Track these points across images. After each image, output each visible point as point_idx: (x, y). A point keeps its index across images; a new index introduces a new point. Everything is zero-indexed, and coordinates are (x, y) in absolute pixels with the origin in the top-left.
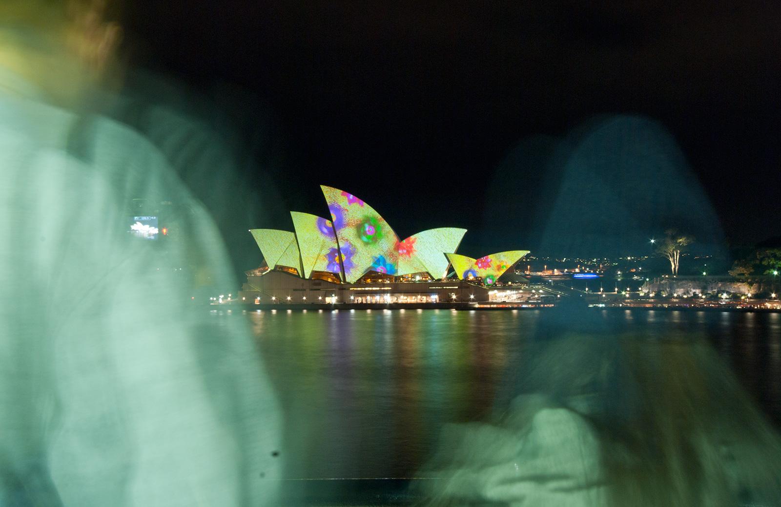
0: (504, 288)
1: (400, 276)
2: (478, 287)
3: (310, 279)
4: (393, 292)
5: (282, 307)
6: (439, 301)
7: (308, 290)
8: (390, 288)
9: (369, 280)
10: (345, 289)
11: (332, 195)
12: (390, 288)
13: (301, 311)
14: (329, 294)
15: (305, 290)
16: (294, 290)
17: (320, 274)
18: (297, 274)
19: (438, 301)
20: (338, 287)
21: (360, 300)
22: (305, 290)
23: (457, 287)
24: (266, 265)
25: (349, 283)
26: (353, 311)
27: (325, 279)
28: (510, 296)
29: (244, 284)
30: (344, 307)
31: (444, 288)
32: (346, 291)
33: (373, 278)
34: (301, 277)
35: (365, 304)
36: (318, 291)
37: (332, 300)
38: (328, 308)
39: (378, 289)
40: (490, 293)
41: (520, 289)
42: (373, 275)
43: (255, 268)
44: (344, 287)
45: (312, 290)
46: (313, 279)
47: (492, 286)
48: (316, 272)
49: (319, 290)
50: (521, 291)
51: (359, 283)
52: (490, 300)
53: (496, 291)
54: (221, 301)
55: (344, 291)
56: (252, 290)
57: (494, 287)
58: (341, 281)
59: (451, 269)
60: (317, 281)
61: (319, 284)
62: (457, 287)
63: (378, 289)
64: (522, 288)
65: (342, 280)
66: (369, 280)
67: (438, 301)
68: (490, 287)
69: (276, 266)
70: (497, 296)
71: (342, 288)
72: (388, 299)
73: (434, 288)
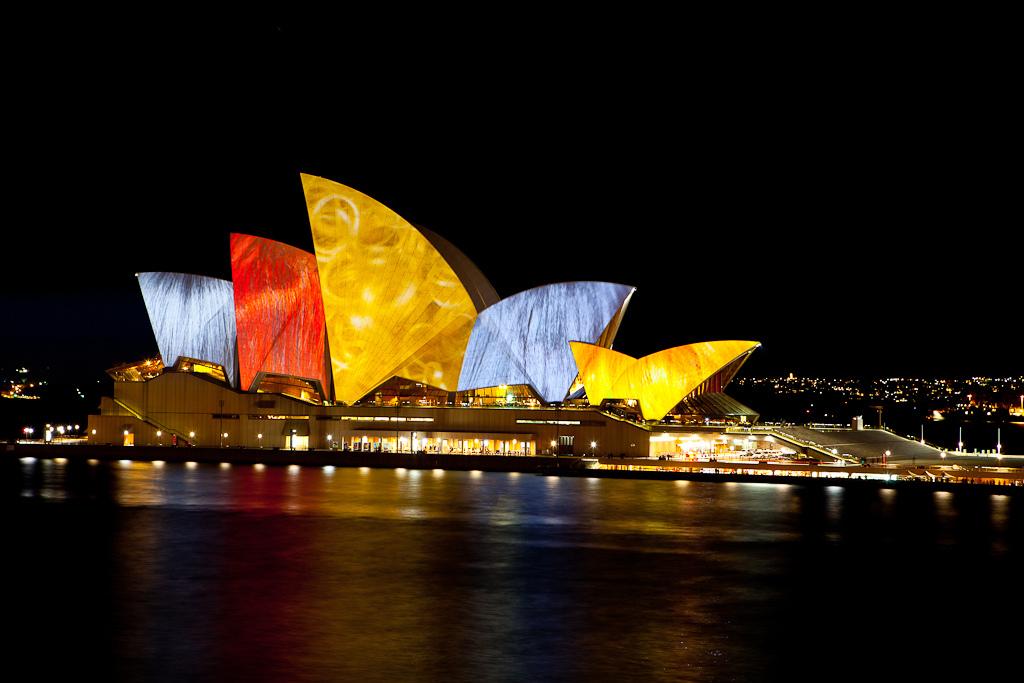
0: (685, 429)
1: (467, 392)
2: (618, 427)
3: (252, 392)
4: (429, 430)
5: (175, 455)
6: (538, 451)
7: (244, 418)
8: (431, 420)
9: (396, 399)
10: (330, 418)
11: (337, 209)
12: (431, 420)
13: (216, 464)
14: (287, 429)
16: (216, 416)
18: (224, 378)
19: (533, 453)
20: (314, 412)
22: (238, 417)
23: (578, 423)
24: (160, 357)
25: (340, 404)
26: (329, 470)
28: (693, 448)
29: (103, 398)
30: (311, 460)
31: (552, 422)
32: (333, 422)
33: (403, 394)
34: (233, 386)
35: (365, 453)
37: (299, 443)
38: (280, 459)
39: (404, 419)
40: (653, 439)
41: (721, 431)
43: (137, 360)
44: (328, 414)
46: (259, 391)
47: (660, 422)
48: (269, 376)
50: (724, 438)
51: (366, 403)
52: (653, 455)
53: (666, 437)
54: (48, 436)
55: (328, 422)
56: (120, 414)
57: (665, 425)
58: (323, 398)
61: (271, 405)
62: (578, 423)
63: (404, 419)
64: (727, 431)
65: (326, 396)
66: (396, 399)
67: (533, 453)
68: (654, 424)
69: (180, 360)
71: (324, 414)
72: (418, 443)
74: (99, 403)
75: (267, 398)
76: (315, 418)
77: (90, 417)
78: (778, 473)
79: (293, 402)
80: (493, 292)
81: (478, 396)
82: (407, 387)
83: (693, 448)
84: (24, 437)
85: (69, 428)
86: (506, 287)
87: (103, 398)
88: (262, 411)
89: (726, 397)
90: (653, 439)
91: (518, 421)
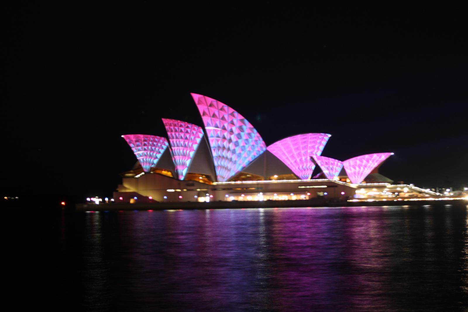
3: (184, 181)
17: (194, 175)
21: (231, 198)
23: (325, 187)
27: (197, 180)
29: (119, 185)
34: (176, 178)
37: (206, 199)
41: (384, 187)
42: (243, 177)
49: (192, 190)
53: (363, 190)
55: (216, 192)
56: (128, 191)
59: (317, 172)
60: (191, 182)
61: (193, 185)
62: (325, 187)
64: (387, 187)
73: (303, 187)
74: (117, 187)
90: (357, 191)
91: (299, 187)
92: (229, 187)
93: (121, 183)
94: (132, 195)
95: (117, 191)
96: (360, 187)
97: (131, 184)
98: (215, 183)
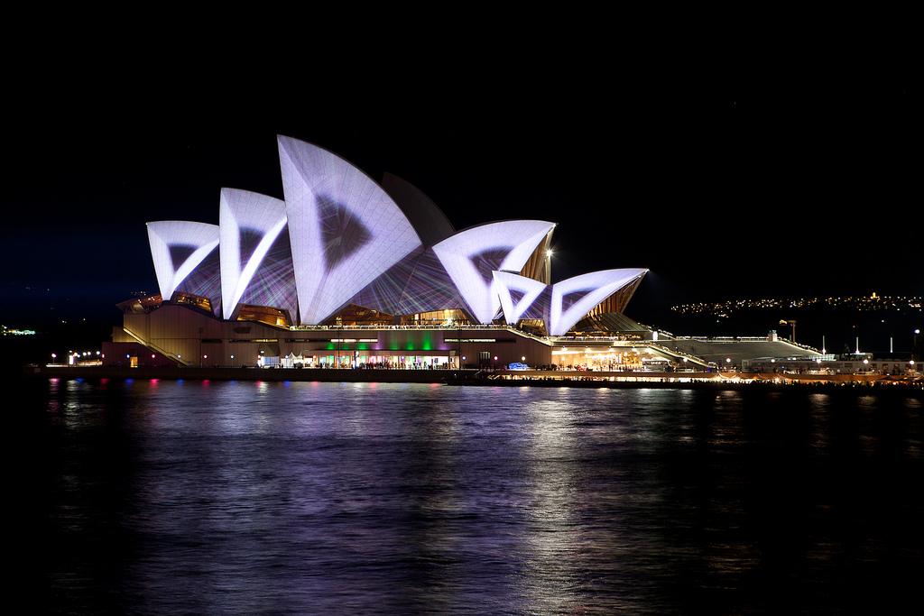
7: (226, 342)
8: (376, 341)
15: (220, 341)
16: (204, 341)
22: (220, 341)
23: (494, 340)
36: (245, 344)
40: (554, 353)
45: (234, 341)
49: (249, 341)
53: (564, 351)
61: (247, 330)
62: (494, 340)
67: (458, 366)
70: (564, 358)
74: (112, 333)
75: (245, 325)
76: (284, 341)
77: (103, 343)
78: (640, 379)
79: (266, 328)
80: (448, 226)
81: (424, 319)
82: (362, 314)
83: (594, 359)
84: (51, 361)
85: (85, 354)
86: (464, 220)
87: (114, 328)
88: (241, 336)
89: (626, 319)
90: (554, 353)
92: (317, 337)
93: (121, 326)
94: (135, 349)
95: (111, 338)
96: (559, 345)
97: (136, 327)
98: (293, 328)
